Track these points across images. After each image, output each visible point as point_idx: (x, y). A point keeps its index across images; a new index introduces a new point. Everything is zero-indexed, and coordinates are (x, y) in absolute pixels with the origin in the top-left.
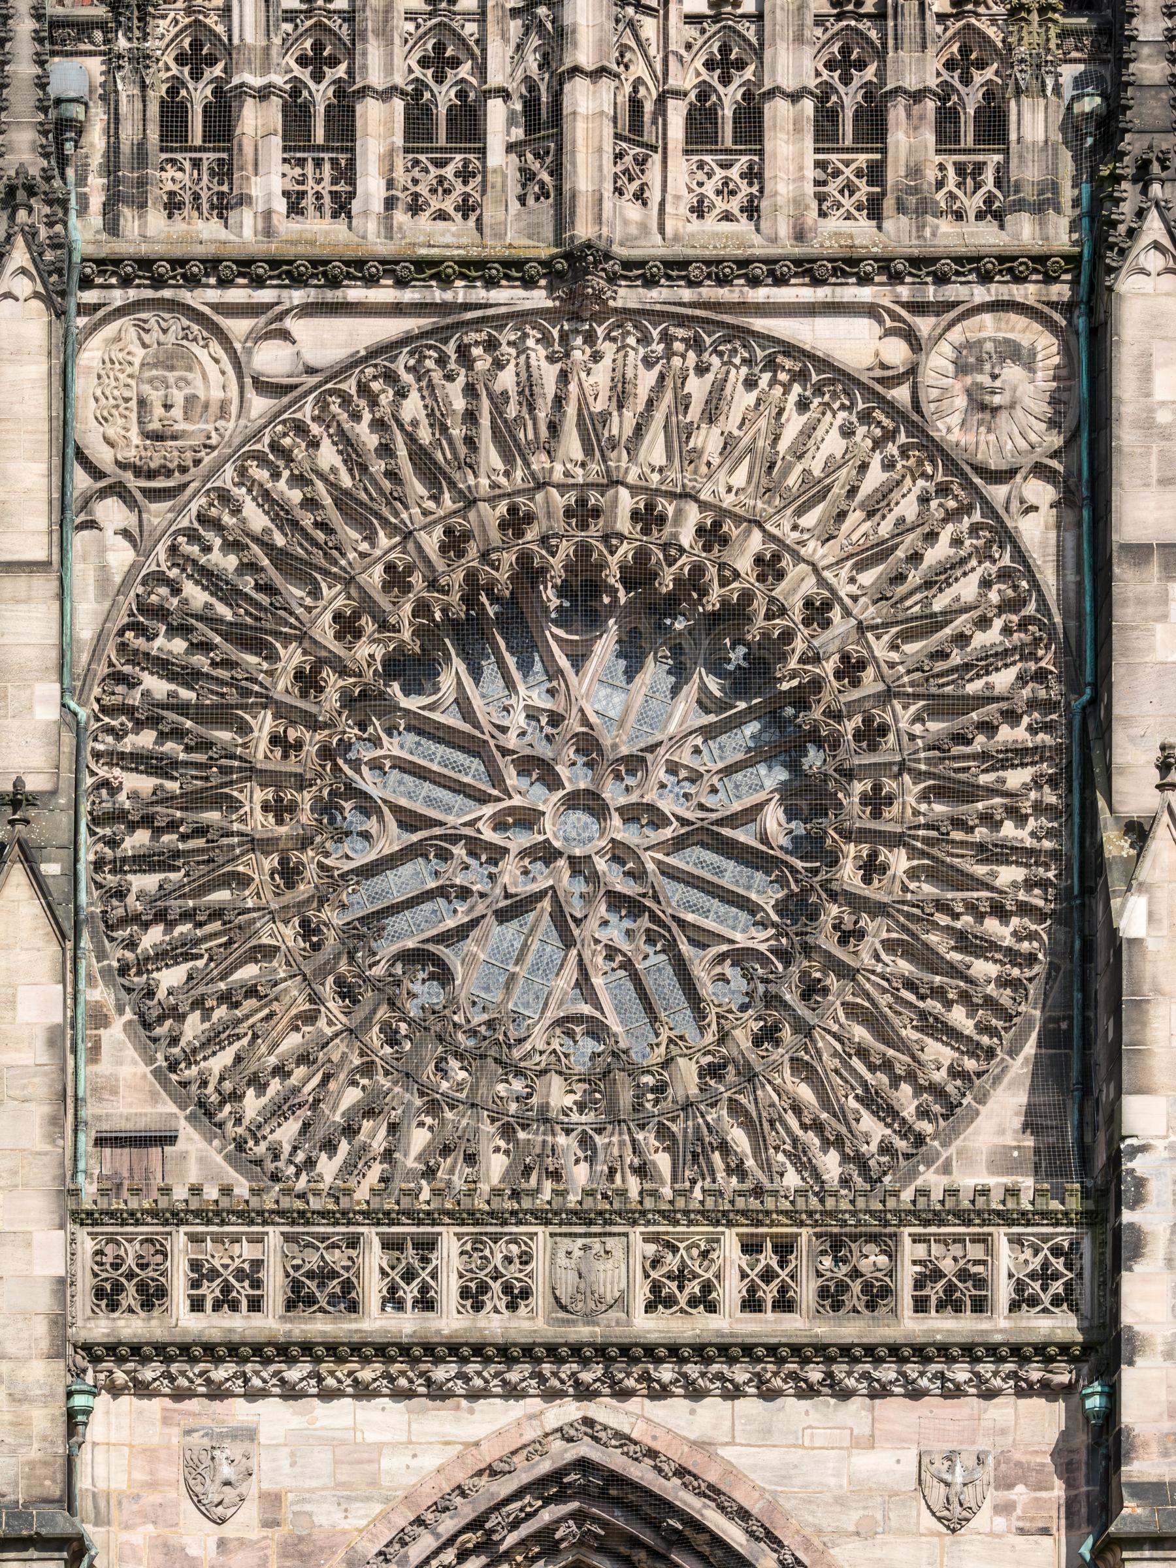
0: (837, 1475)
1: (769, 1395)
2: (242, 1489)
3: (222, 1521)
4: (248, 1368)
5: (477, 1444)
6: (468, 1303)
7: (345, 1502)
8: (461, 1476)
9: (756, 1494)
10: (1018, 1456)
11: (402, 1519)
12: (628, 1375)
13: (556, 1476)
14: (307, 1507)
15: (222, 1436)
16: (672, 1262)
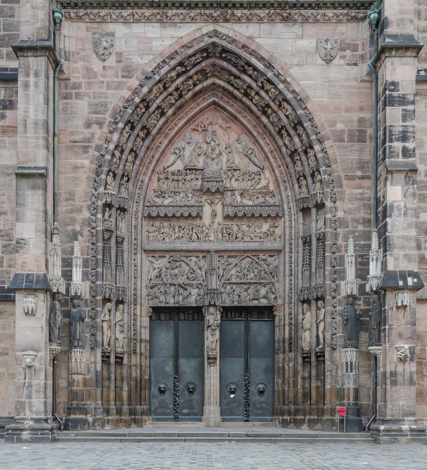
1: (271, 21)
2: (111, 50)
3: (104, 60)
5: (182, 38)
8: (176, 47)
9: (267, 53)
10: (347, 41)
14: (130, 57)
15: (104, 35)
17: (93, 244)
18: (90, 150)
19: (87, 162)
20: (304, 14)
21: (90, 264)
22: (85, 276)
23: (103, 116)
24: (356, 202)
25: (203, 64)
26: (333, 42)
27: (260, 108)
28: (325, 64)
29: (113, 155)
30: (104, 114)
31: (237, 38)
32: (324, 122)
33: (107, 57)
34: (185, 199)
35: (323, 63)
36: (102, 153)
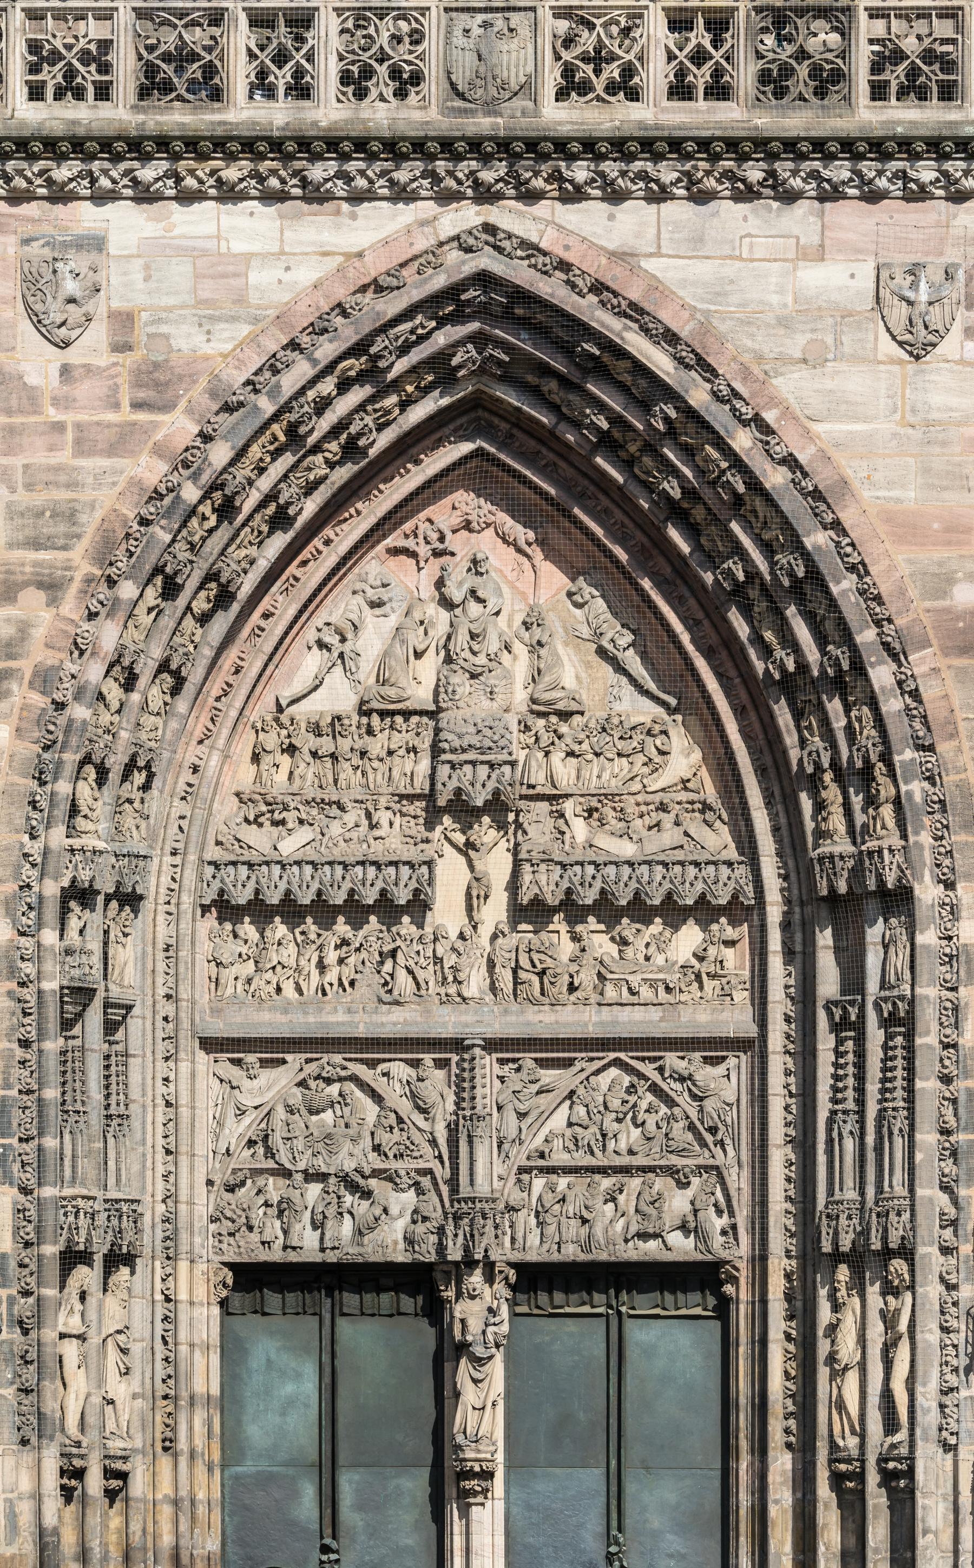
0: (781, 291)
1: (701, 197)
2: (89, 307)
3: (65, 345)
4: (96, 166)
5: (360, 255)
6: (350, 90)
8: (341, 293)
9: (686, 314)
11: (273, 342)
12: (536, 174)
13: (452, 292)
14: (164, 329)
15: (65, 245)
16: (587, 41)
17: (25, 1044)
18: (15, 687)
21: (15, 1125)
23: (61, 555)
28: (906, 357)
30: (65, 548)
33: (78, 331)
36: (58, 697)
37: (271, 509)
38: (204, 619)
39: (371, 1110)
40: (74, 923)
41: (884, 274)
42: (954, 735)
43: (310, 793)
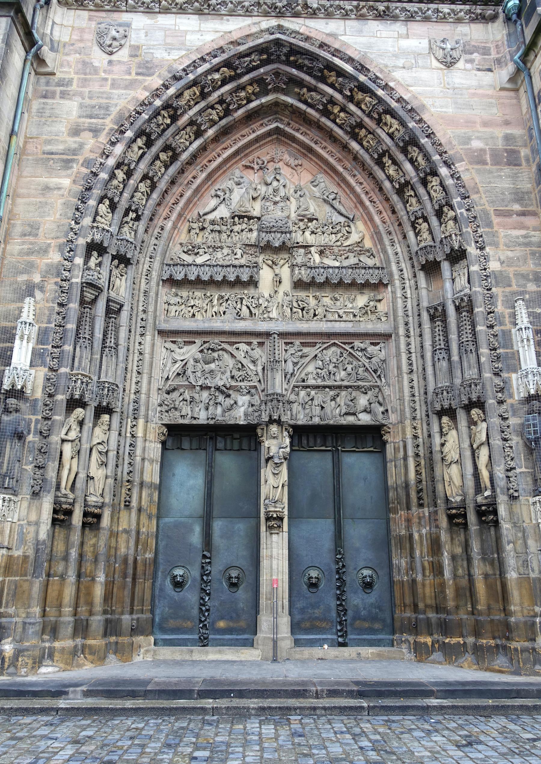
1: (361, 17)
3: (111, 53)
5: (230, 32)
7: (169, 48)
8: (222, 43)
9: (357, 52)
10: (473, 43)
11: (195, 57)
14: (151, 51)
17: (61, 305)
18: (75, 165)
19: (66, 182)
20: (408, 9)
21: (51, 339)
22: (37, 358)
23: (101, 121)
24: (518, 248)
25: (262, 70)
26: (454, 44)
27: (349, 129)
29: (113, 176)
30: (103, 118)
31: (312, 35)
32: (452, 139)
34: (229, 254)
35: (442, 66)
36: (94, 170)
37: (195, 128)
38: (167, 167)
39: (231, 362)
40: (93, 262)
41: (432, 41)
42: (478, 192)
43: (209, 244)
